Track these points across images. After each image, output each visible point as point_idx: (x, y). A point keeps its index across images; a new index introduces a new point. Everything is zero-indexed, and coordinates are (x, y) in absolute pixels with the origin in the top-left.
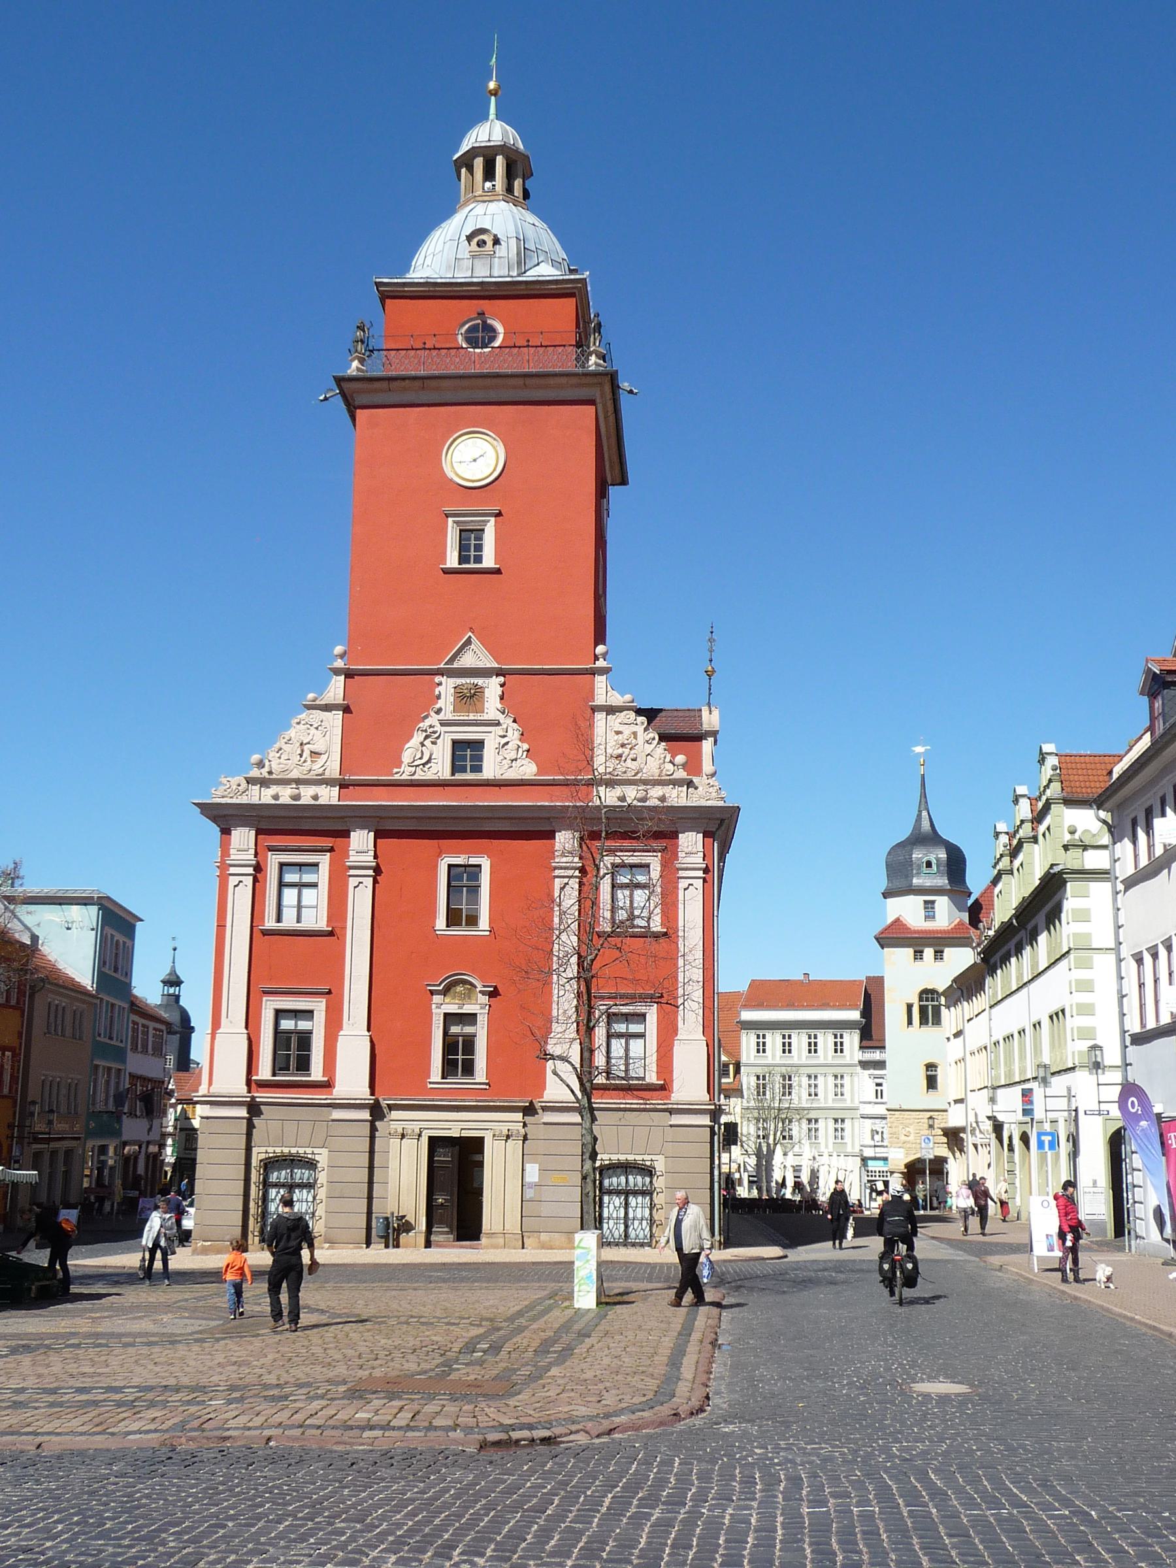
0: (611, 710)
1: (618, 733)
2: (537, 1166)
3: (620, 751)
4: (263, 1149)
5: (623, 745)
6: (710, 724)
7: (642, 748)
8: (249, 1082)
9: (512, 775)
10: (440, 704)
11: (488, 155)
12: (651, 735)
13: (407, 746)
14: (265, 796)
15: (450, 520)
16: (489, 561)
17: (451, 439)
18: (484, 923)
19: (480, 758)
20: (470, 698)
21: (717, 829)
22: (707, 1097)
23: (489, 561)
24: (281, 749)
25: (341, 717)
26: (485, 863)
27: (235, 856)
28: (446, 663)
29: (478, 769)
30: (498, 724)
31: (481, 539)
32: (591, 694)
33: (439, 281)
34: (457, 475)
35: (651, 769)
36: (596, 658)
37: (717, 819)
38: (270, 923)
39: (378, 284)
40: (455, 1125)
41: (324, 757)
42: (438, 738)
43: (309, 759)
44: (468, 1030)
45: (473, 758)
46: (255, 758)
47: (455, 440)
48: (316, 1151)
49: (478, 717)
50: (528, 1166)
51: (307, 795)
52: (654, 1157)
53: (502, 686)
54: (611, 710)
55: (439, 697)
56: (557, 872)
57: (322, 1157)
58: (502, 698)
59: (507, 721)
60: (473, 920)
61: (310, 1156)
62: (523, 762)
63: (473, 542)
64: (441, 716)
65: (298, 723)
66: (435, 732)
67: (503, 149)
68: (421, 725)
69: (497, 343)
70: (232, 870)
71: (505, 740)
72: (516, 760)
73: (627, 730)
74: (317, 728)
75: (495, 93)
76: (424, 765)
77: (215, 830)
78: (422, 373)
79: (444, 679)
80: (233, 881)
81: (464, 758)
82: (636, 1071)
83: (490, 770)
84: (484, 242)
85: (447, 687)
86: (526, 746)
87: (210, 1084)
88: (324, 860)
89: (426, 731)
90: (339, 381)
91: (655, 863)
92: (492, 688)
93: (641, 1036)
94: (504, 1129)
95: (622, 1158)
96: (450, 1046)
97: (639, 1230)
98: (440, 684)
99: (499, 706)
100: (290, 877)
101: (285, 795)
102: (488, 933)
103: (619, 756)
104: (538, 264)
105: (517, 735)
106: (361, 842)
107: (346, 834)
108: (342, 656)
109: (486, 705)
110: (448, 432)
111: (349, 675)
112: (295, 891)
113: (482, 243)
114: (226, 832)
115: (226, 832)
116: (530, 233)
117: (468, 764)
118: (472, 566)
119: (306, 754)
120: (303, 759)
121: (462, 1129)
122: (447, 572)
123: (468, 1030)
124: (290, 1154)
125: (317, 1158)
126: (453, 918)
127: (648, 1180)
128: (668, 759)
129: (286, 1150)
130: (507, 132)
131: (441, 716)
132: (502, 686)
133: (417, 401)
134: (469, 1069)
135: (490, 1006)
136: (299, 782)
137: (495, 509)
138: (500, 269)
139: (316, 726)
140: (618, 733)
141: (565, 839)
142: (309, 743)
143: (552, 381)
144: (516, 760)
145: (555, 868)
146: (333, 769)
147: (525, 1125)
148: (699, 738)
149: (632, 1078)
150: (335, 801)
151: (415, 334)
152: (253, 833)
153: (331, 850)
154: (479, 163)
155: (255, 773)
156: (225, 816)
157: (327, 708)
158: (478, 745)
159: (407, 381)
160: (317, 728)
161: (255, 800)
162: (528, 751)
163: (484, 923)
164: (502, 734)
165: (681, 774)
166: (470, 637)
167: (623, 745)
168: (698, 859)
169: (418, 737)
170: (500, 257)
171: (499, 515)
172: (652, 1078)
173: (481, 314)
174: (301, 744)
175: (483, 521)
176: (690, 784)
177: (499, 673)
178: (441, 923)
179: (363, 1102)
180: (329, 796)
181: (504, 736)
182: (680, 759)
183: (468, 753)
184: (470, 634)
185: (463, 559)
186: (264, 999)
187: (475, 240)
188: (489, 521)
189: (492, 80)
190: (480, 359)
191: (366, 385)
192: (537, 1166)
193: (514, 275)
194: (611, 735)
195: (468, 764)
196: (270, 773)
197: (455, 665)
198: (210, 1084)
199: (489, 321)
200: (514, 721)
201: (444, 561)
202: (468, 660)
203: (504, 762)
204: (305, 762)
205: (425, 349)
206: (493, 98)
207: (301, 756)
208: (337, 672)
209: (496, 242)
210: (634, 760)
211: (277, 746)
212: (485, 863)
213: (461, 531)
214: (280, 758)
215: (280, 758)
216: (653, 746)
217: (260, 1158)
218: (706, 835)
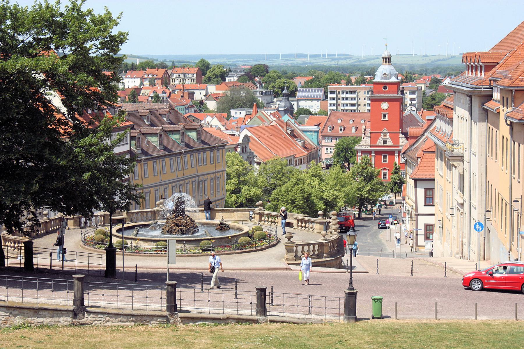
0: (402, 137)
9: (390, 145)
18: (387, 162)
20: (385, 136)
23: (387, 119)
54: (402, 137)
60: (386, 161)
83: (388, 144)
85: (382, 135)
92: (388, 135)
96: (384, 175)
111: (371, 133)
122: (382, 120)
146: (369, 144)
163: (387, 162)
169: (379, 140)
178: (382, 162)
180: (369, 148)
185: (384, 118)
202: (385, 131)
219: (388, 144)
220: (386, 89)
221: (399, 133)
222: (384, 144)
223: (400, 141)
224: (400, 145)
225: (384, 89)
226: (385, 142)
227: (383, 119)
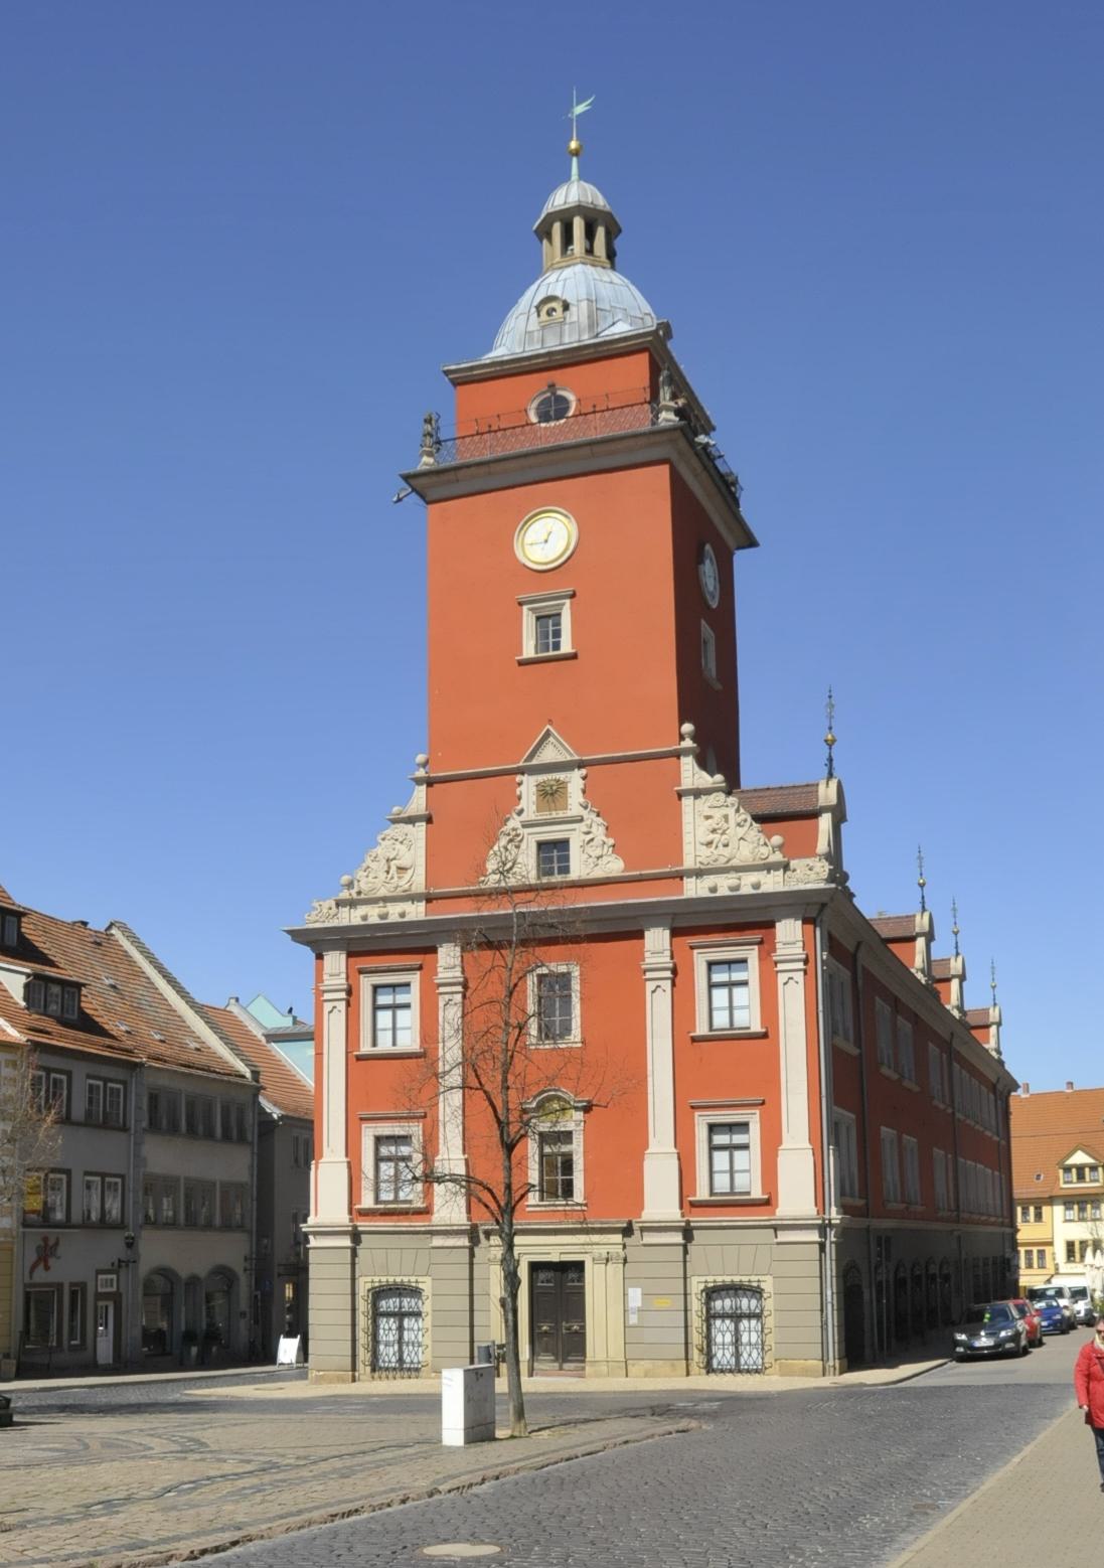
0: (697, 793)
1: (708, 818)
2: (639, 1291)
3: (711, 837)
4: (369, 1279)
5: (714, 831)
6: (826, 797)
8: (350, 1212)
10: (523, 804)
11: (565, 218)
12: (743, 817)
14: (352, 917)
15: (525, 608)
16: (566, 647)
17: (522, 523)
18: (576, 1035)
19: (567, 859)
20: (551, 795)
21: (819, 914)
22: (678, 1212)
23: (566, 647)
24: (368, 867)
25: (424, 828)
26: (576, 972)
27: (328, 982)
28: (525, 761)
29: (565, 870)
30: (581, 820)
31: (559, 624)
32: (678, 780)
33: (505, 358)
34: (532, 561)
35: (745, 853)
36: (682, 738)
37: (816, 903)
38: (366, 1048)
39: (447, 373)
40: (555, 1249)
41: (410, 872)
42: (521, 841)
43: (396, 876)
44: (565, 1149)
46: (345, 879)
47: (526, 523)
48: (420, 1279)
49: (561, 814)
50: (631, 1291)
51: (394, 912)
52: (762, 1278)
53: (584, 778)
54: (697, 793)
55: (520, 798)
56: (649, 975)
57: (426, 1285)
58: (584, 792)
59: (590, 817)
61: (414, 1285)
63: (551, 628)
64: (524, 817)
65: (383, 839)
66: (518, 835)
67: (579, 209)
68: (504, 829)
69: (571, 413)
70: (327, 996)
72: (601, 856)
73: (718, 814)
74: (401, 843)
75: (576, 153)
77: (308, 953)
78: (488, 456)
79: (525, 778)
80: (327, 1007)
81: (551, 860)
82: (741, 1181)
83: (579, 869)
84: (554, 310)
85: (528, 786)
86: (611, 841)
87: (316, 1214)
88: (415, 979)
89: (509, 834)
90: (407, 478)
91: (752, 955)
92: (575, 780)
93: (745, 1147)
94: (603, 1251)
95: (728, 1279)
97: (751, 1357)
98: (520, 784)
99: (582, 800)
100: (383, 999)
101: (373, 914)
102: (579, 1045)
103: (709, 844)
104: (614, 324)
105: (602, 830)
106: (448, 956)
107: (433, 950)
108: (425, 765)
109: (570, 801)
110: (522, 517)
112: (389, 1013)
114: (320, 957)
115: (320, 957)
116: (605, 291)
117: (556, 866)
118: (551, 653)
119: (393, 869)
120: (390, 876)
121: (561, 1253)
123: (565, 1149)
124: (395, 1283)
125: (420, 1286)
126: (546, 1032)
127: (754, 1302)
128: (762, 842)
129: (391, 1279)
130: (585, 190)
131: (524, 817)
132: (584, 778)
133: (486, 487)
134: (568, 1191)
135: (585, 1122)
136: (386, 900)
137: (569, 590)
138: (573, 334)
139: (401, 839)
140: (708, 818)
141: (657, 940)
142: (394, 859)
144: (601, 856)
145: (645, 971)
146: (419, 883)
147: (624, 1246)
148: (814, 815)
149: (716, 1194)
150: (422, 917)
152: (343, 956)
153: (420, 968)
154: (557, 228)
155: (345, 895)
156: (317, 941)
157: (411, 820)
158: (563, 845)
159: (473, 469)
160: (401, 843)
161: (345, 922)
162: (614, 846)
163: (576, 1035)
164: (586, 830)
165: (778, 857)
166: (548, 730)
167: (714, 831)
168: (798, 951)
170: (571, 323)
171: (573, 596)
172: (757, 1193)
173: (552, 386)
174: (388, 860)
175: (558, 605)
176: (786, 867)
177: (581, 765)
179: (460, 1228)
180: (416, 912)
181: (588, 833)
182: (777, 840)
183: (555, 853)
184: (548, 727)
186: (363, 1126)
187: (545, 309)
188: (564, 604)
189: (571, 139)
190: (553, 433)
191: (435, 479)
192: (639, 1291)
193: (587, 339)
194: (700, 820)
195: (556, 866)
196: (359, 893)
197: (535, 762)
198: (316, 1214)
199: (560, 393)
200: (598, 815)
202: (550, 754)
203: (590, 860)
204: (392, 878)
205: (490, 432)
206: (575, 160)
207: (388, 872)
208: (418, 781)
209: (566, 307)
210: (726, 845)
211: (364, 865)
212: (576, 972)
213: (538, 618)
214: (367, 876)
215: (367, 876)
216: (746, 828)
217: (367, 1288)
218: (805, 921)
219: (579, 869)
221: (678, 754)
224: (689, 863)
226: (553, 852)
227: (529, 651)
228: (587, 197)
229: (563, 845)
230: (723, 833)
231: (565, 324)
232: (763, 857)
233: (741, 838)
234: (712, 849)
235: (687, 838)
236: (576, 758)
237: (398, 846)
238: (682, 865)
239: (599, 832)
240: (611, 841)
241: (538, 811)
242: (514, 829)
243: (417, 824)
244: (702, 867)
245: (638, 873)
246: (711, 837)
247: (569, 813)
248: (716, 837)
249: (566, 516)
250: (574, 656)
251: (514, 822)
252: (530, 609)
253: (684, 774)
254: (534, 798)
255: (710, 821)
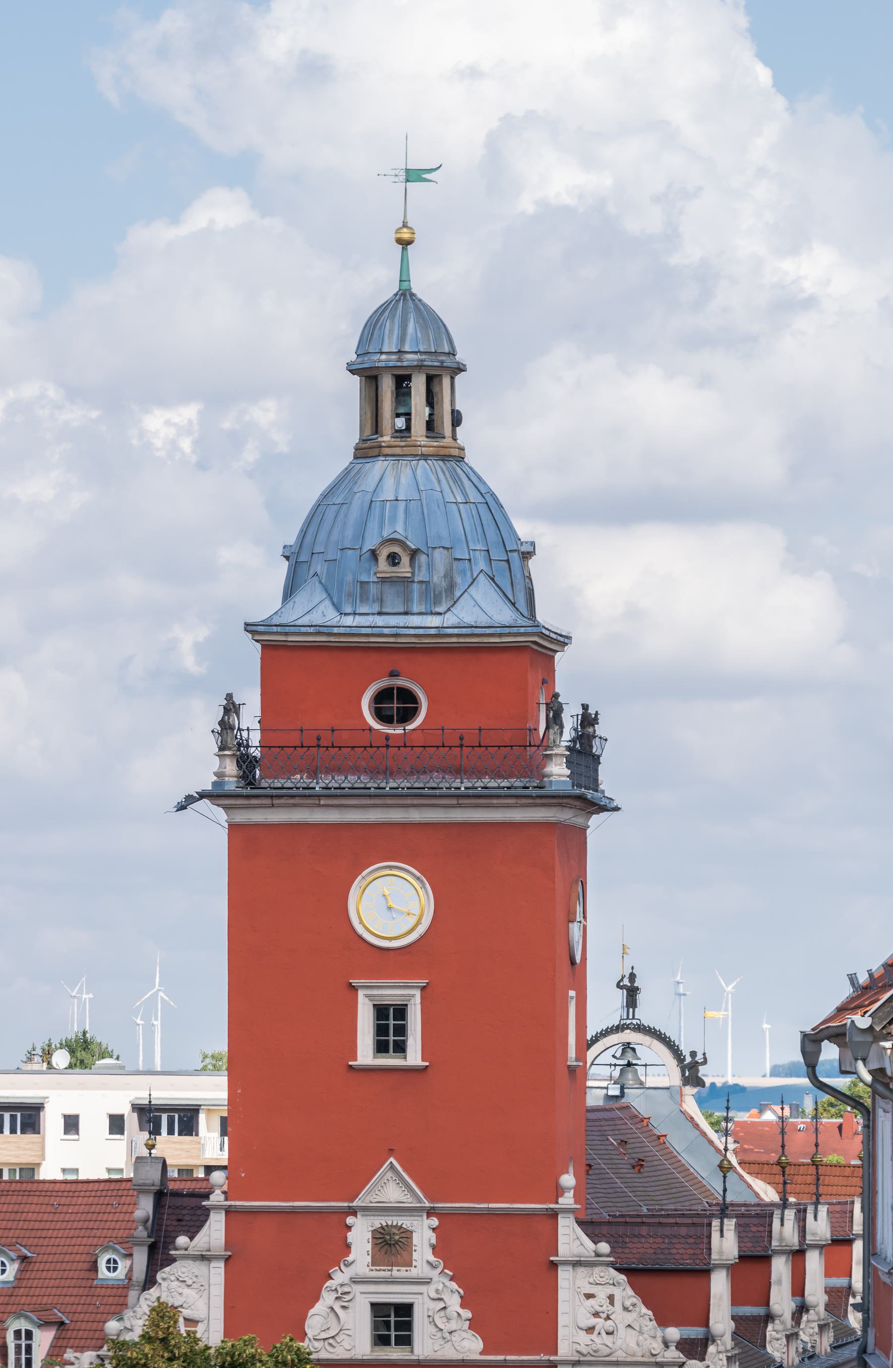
0: (577, 1264)
1: (589, 1296)
3: (593, 1321)
7: (620, 1317)
13: (309, 1314)
16: (414, 1056)
29: (406, 1341)
30: (427, 1282)
45: (399, 1326)
62: (464, 1335)
63: (392, 1022)
71: (442, 1305)
76: (333, 1337)
89: (336, 1290)
98: (349, 1228)
99: (432, 1258)
103: (590, 1330)
109: (415, 1256)
113: (393, 559)
117: (393, 1334)
140: (589, 1296)
143: (495, 801)
151: (304, 728)
154: (387, 385)
158: (405, 1310)
164: (436, 1296)
167: (596, 1314)
170: (421, 582)
177: (430, 1213)
181: (441, 1299)
184: (392, 1159)
185: (381, 1048)
195: (393, 1334)
201: (352, 1050)
209: (414, 554)
220: (407, 715)
222: (381, 1340)
223: (562, 1295)
225: (382, 716)
228: (430, 346)
229: (405, 1310)
230: (608, 1318)
231: (413, 582)
232: (654, 1352)
233: (629, 1326)
234: (594, 1336)
235: (562, 1320)
236: (427, 1204)
237: (186, 1291)
238: (556, 1353)
239: (454, 1302)
240: (467, 1314)
241: (372, 1265)
242: (342, 1285)
243: (213, 1264)
244: (582, 1359)
245: (501, 1358)
246: (593, 1321)
247: (414, 1272)
248: (599, 1322)
249: (418, 879)
250: (423, 1070)
251: (340, 1277)
252: (366, 996)
253: (561, 1239)
254: (369, 1247)
255: (591, 1301)
